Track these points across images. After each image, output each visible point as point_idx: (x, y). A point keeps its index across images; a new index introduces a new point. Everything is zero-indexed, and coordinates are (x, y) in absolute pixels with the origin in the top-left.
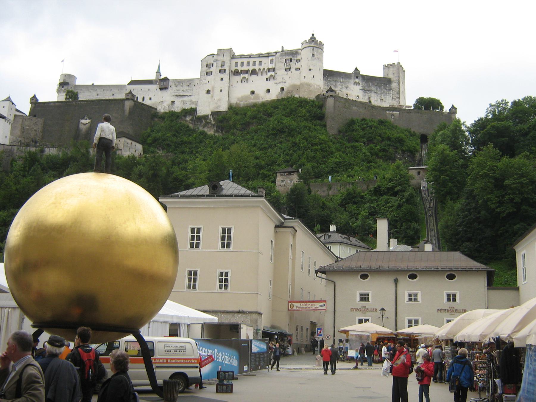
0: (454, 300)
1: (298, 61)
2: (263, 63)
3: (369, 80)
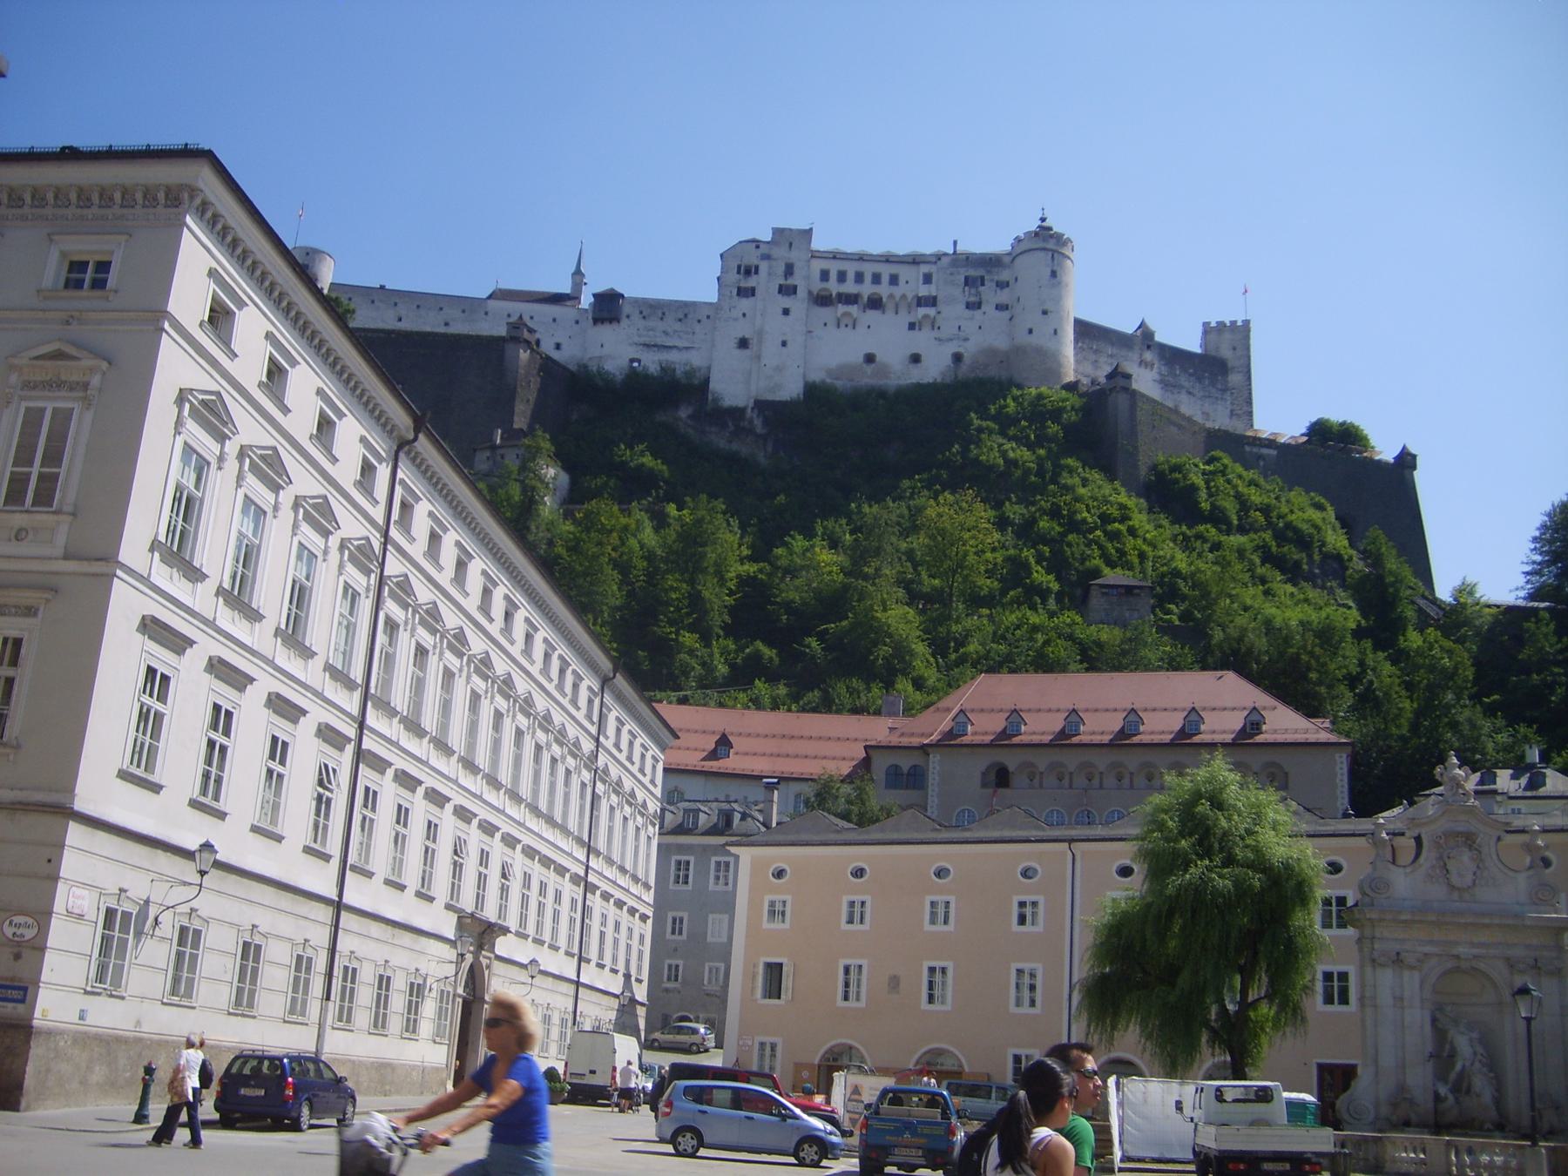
1: (1002, 285)
2: (902, 281)
3: (1172, 356)
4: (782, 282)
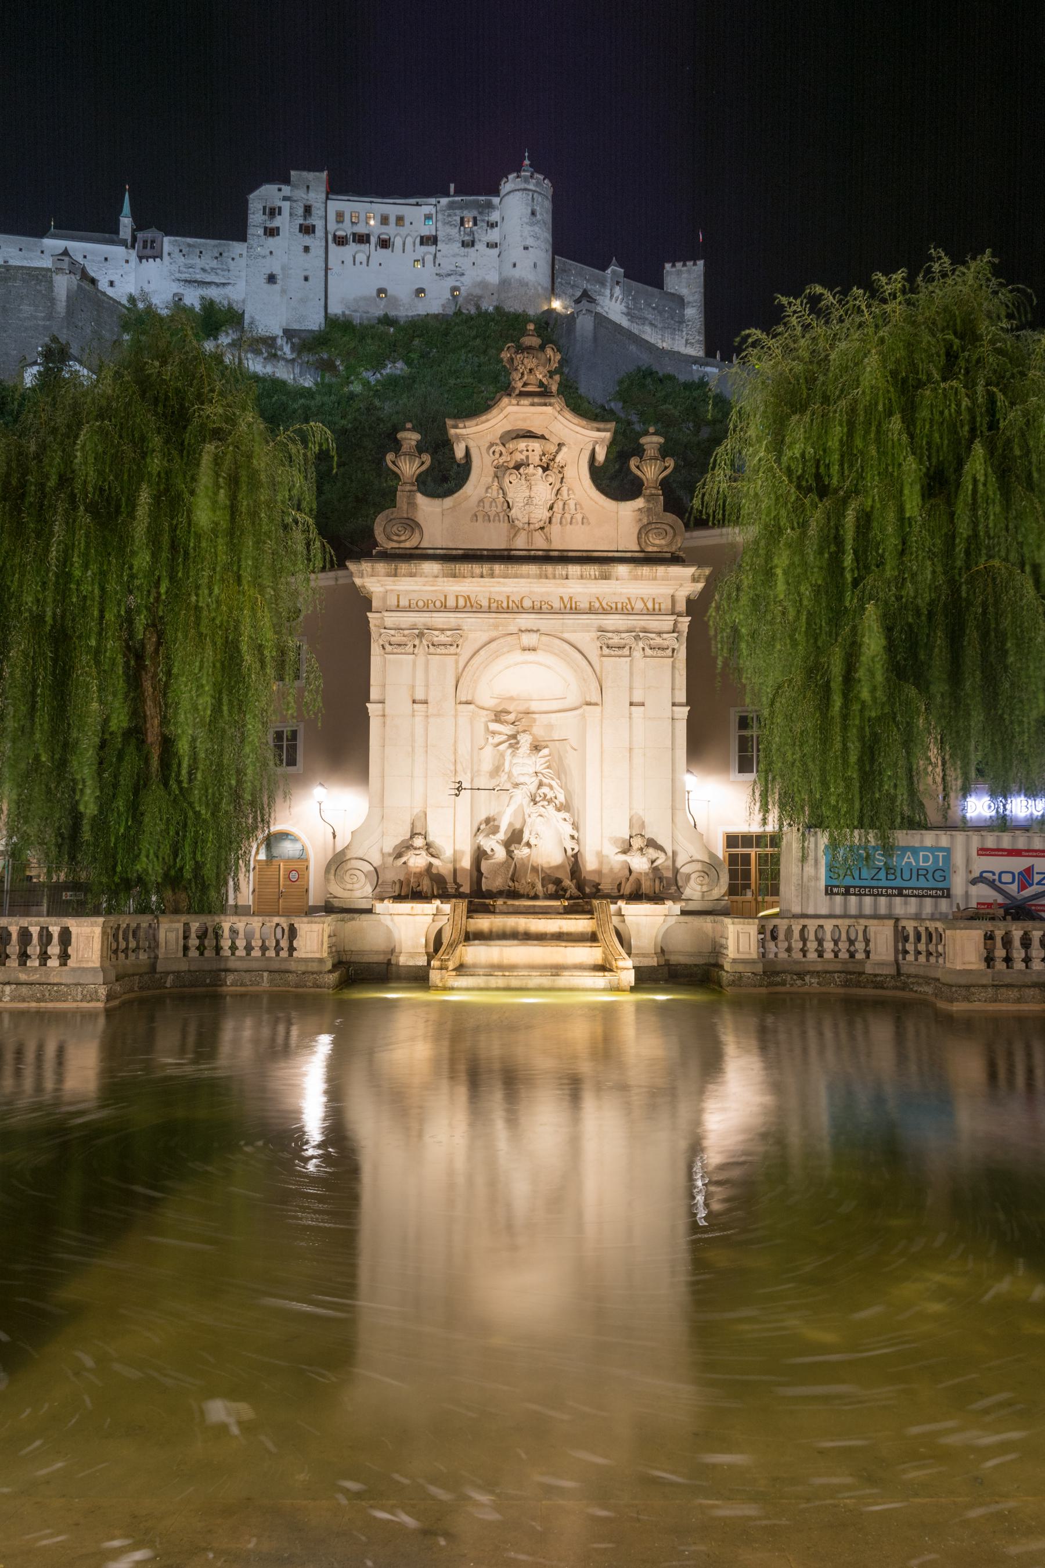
1: (492, 225)
2: (407, 222)
4: (302, 222)
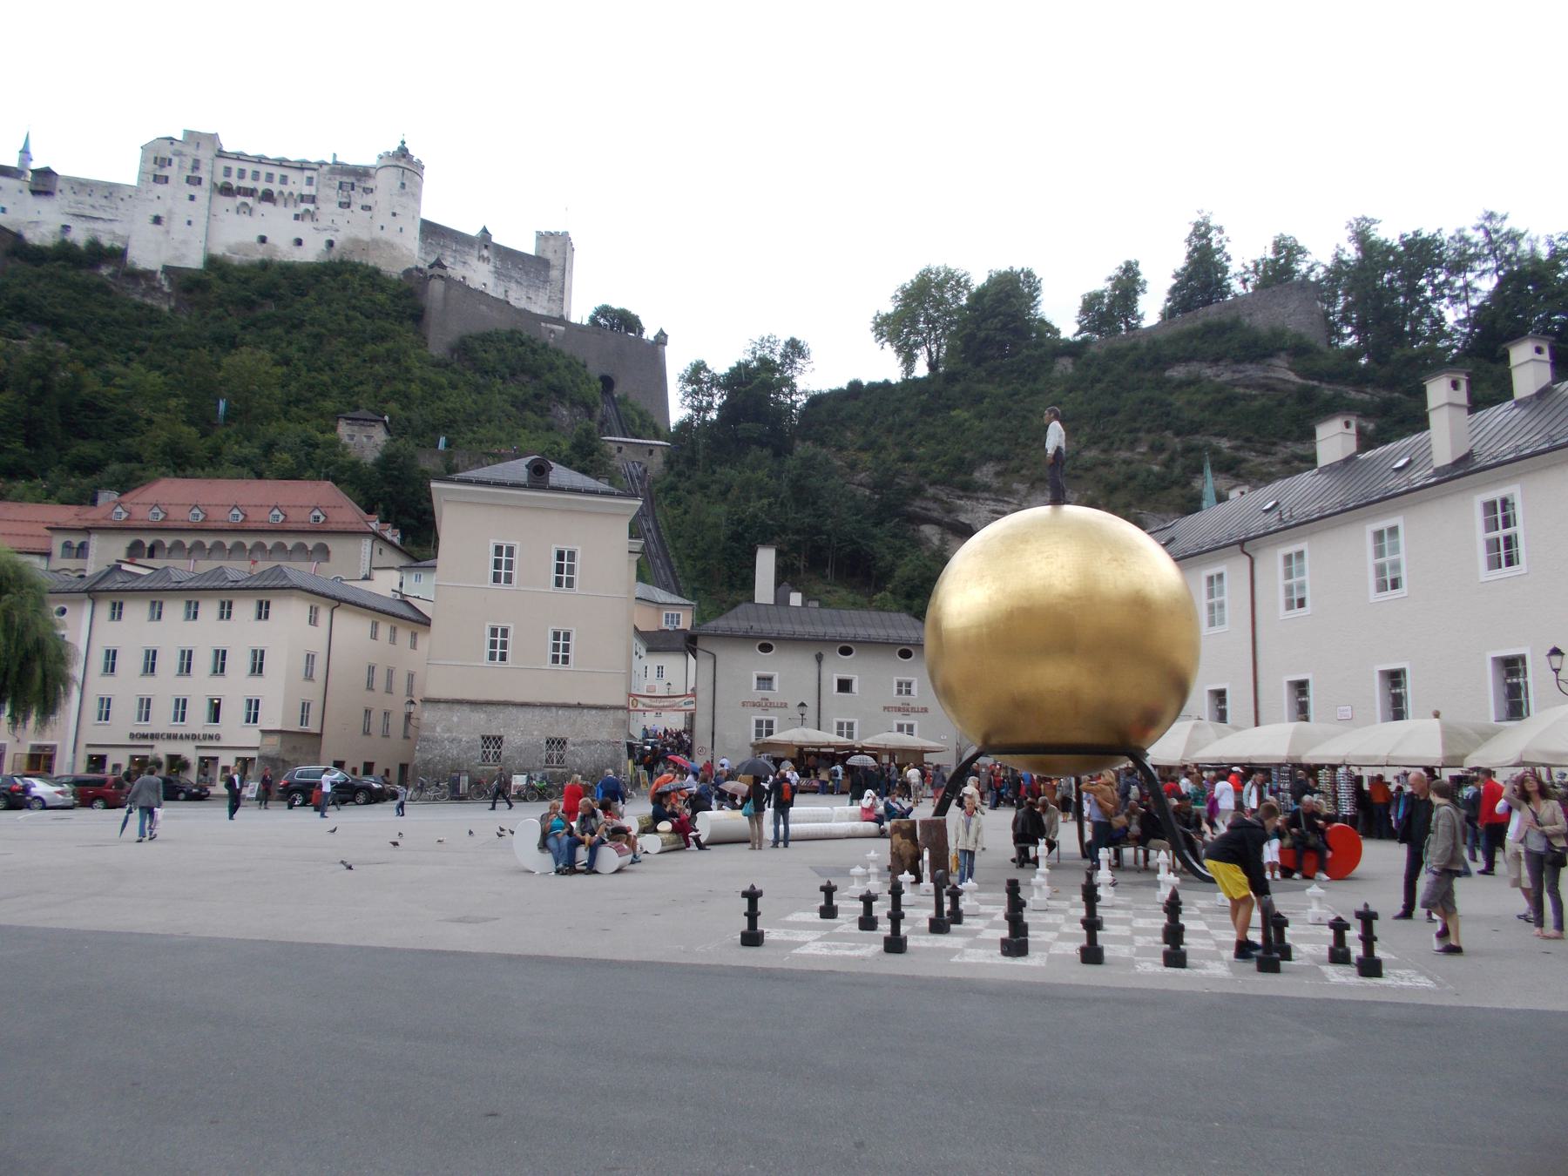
0: (909, 692)
2: (290, 182)
3: (507, 256)
